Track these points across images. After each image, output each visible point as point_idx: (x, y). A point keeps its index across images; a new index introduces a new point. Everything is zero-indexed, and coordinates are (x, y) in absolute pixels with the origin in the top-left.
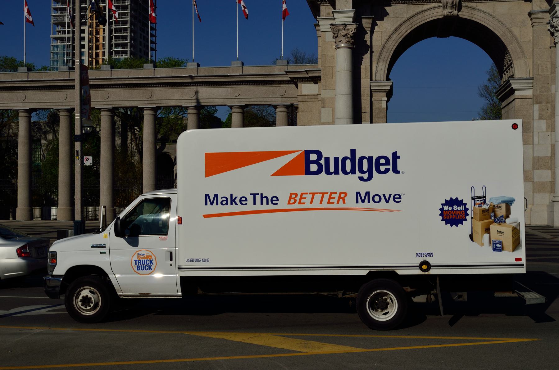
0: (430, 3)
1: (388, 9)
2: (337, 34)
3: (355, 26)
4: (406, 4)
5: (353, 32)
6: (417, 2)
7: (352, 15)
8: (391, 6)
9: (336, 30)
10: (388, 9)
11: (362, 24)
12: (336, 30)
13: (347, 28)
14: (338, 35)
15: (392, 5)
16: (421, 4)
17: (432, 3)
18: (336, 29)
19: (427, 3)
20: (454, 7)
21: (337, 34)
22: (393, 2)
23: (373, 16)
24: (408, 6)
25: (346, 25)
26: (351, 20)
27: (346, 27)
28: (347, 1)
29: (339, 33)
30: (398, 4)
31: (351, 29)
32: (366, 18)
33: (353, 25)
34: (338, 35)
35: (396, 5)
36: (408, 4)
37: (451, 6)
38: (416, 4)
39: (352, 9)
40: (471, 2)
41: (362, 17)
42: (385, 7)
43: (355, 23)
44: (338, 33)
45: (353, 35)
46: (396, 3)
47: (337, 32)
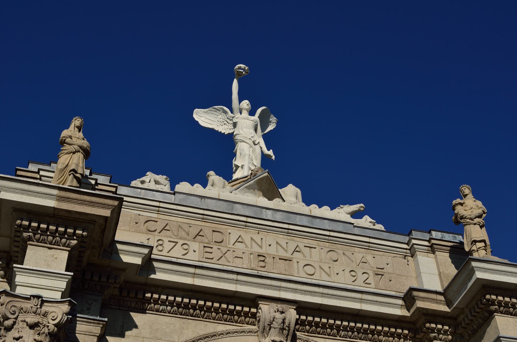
0: (232, 323)
1: (137, 317)
2: (14, 320)
3: (66, 308)
4: (179, 316)
5: (56, 322)
6: (204, 314)
7: (62, 285)
8: (146, 313)
9: (13, 308)
10: (137, 317)
11: (75, 333)
12: (13, 308)
13: (45, 308)
14: (14, 323)
15: (147, 312)
16: (212, 321)
17: (235, 324)
18: (15, 306)
19: (226, 321)
20: (285, 332)
21: (14, 320)
22: (153, 305)
23: (106, 319)
24: (184, 320)
25: (43, 302)
26: (57, 296)
27: (41, 308)
28: (55, 257)
29: (19, 319)
30: (163, 314)
31: (53, 314)
32: (89, 321)
33: (59, 305)
34: (14, 323)
35: (158, 313)
36: (185, 317)
37: (280, 328)
38: (201, 319)
39: (66, 271)
40: (314, 335)
41: (78, 315)
42: (132, 314)
43: (69, 299)
44: (16, 318)
45: (56, 329)
46: (157, 311)
47: (15, 316)
